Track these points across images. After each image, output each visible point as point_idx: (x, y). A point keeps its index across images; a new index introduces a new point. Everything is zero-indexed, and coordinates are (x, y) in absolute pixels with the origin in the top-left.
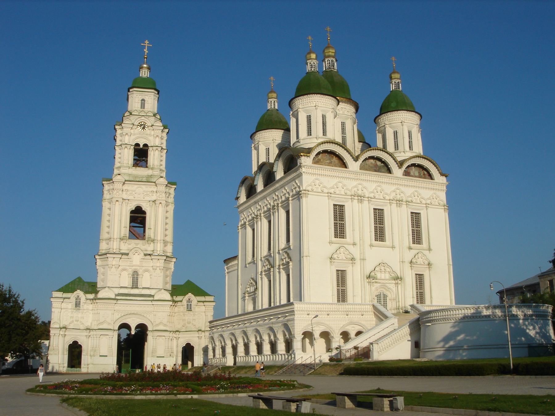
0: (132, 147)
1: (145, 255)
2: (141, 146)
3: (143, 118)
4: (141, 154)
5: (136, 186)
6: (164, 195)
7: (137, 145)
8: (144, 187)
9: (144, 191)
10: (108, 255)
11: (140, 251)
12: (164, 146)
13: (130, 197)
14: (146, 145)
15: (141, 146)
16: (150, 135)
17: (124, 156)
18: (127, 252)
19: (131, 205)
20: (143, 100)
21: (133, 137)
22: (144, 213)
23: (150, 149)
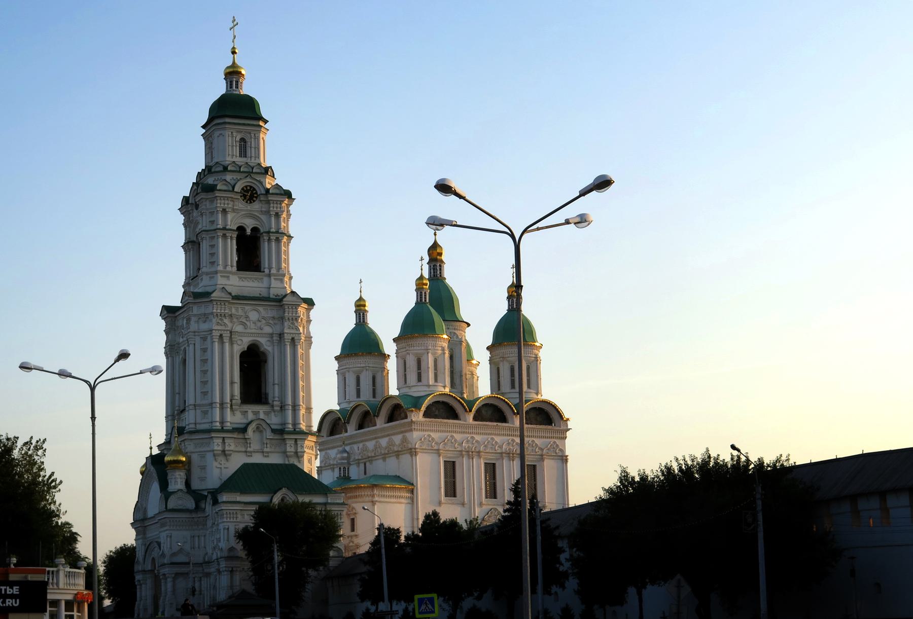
0: (235, 235)
1: (274, 431)
2: (249, 232)
3: (248, 179)
5: (247, 308)
7: (241, 229)
8: (261, 309)
9: (264, 318)
10: (213, 435)
11: (264, 425)
13: (239, 328)
14: (255, 230)
15: (249, 232)
18: (242, 426)
19: (239, 342)
20: (243, 140)
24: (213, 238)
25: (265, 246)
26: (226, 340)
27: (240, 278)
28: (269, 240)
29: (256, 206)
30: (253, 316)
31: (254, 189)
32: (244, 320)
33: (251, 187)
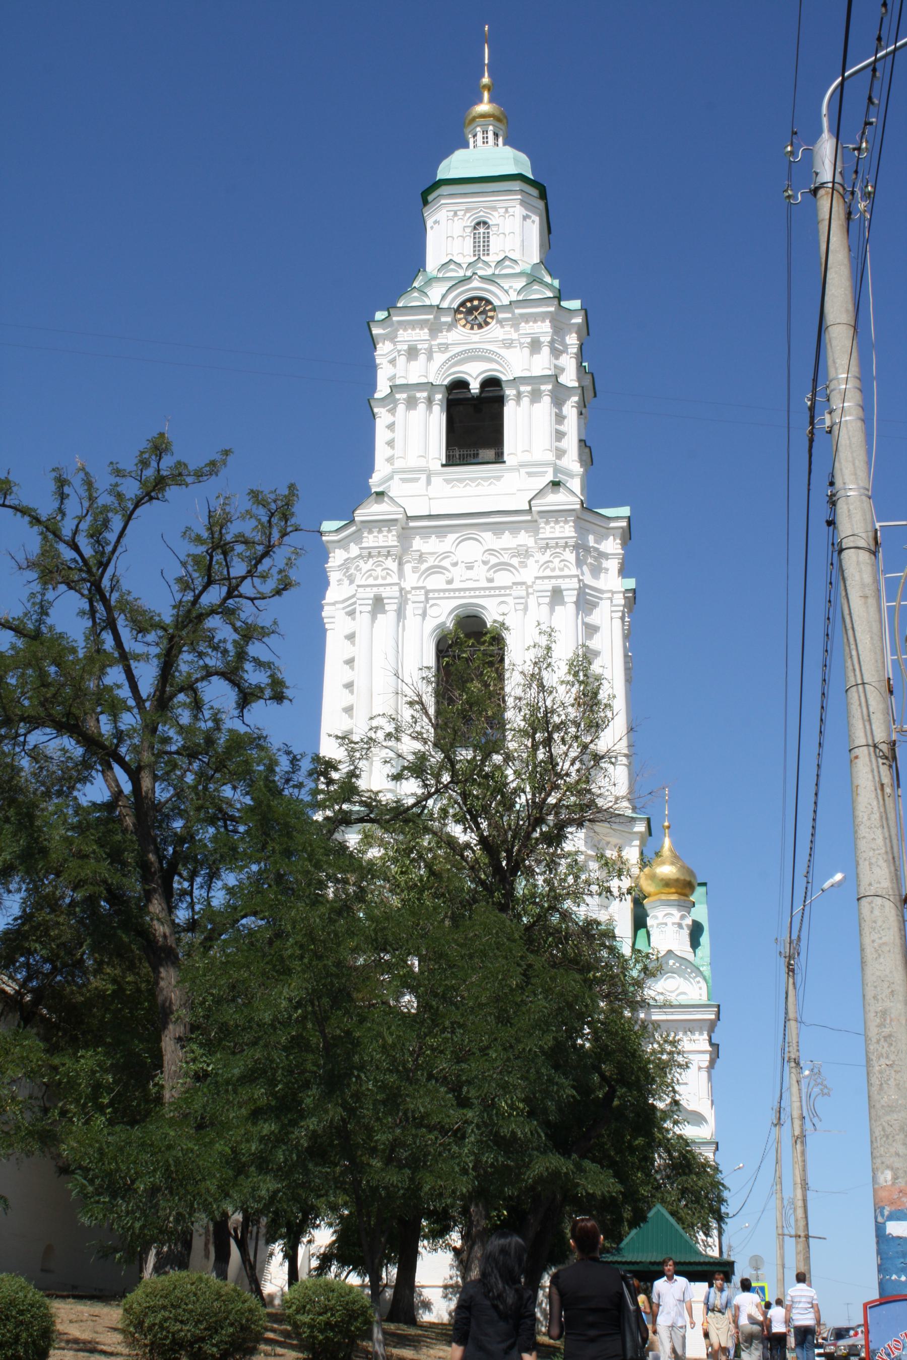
2: (475, 387)
4: (474, 422)
5: (451, 537)
6: (570, 556)
7: (460, 385)
8: (487, 536)
12: (570, 378)
13: (436, 582)
14: (492, 384)
15: (475, 387)
16: (508, 344)
17: (409, 437)
21: (439, 358)
22: (498, 640)
23: (509, 392)
24: (392, 411)
25: (510, 412)
26: (391, 607)
27: (448, 481)
28: (519, 396)
29: (494, 331)
30: (470, 551)
31: (488, 302)
32: (446, 563)
33: (481, 299)
